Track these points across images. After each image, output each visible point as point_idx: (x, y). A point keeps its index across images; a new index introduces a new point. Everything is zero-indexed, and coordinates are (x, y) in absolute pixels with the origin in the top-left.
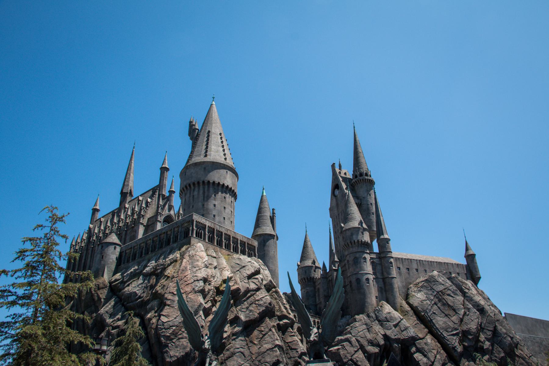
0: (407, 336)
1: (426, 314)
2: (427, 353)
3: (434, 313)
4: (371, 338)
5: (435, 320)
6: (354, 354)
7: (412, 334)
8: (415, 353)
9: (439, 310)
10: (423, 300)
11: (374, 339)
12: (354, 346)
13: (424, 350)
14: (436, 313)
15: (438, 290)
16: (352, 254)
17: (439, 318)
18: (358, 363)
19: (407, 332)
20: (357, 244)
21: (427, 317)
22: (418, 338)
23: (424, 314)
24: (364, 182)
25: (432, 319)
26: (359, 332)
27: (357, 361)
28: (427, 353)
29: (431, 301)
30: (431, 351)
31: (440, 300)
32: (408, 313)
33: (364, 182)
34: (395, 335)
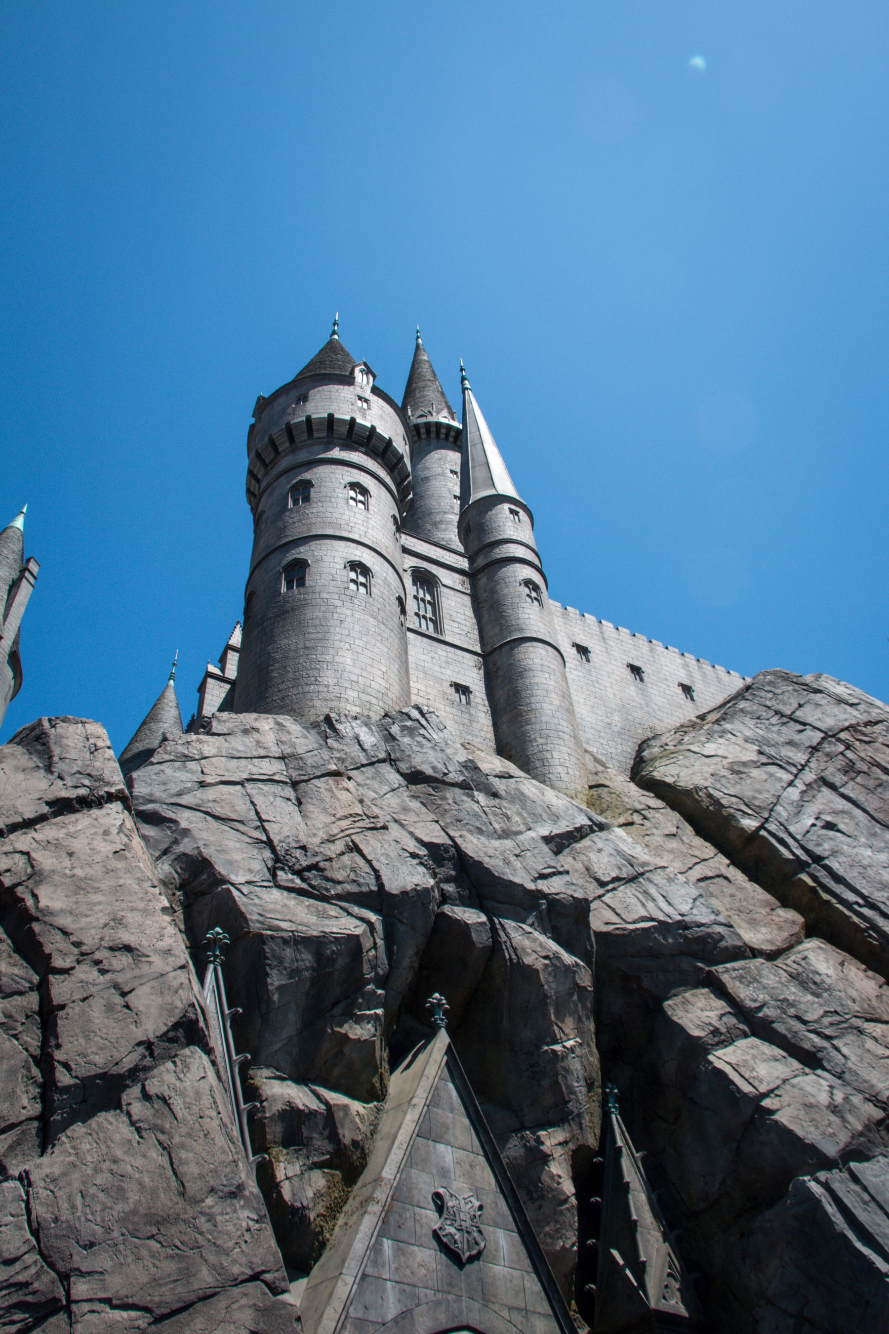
0: (643, 919)
1: (772, 827)
2: (828, 1038)
3: (829, 826)
4: (313, 842)
5: (842, 859)
6: (28, 824)
7: (685, 908)
8: (724, 1039)
9: (858, 812)
10: (744, 764)
11: (339, 846)
12: (59, 767)
13: (799, 1018)
14: (841, 826)
15: (828, 723)
16: (283, 478)
17: (869, 852)
18: (42, 892)
19: (646, 892)
20: (324, 434)
21: (782, 841)
22: (730, 942)
23: (762, 827)
24: (433, 435)
25: (818, 851)
26: (202, 784)
27: (36, 875)
28: (828, 1038)
29: (794, 771)
30: (861, 1032)
31: (850, 769)
32: (645, 818)
33: (433, 435)
34: (543, 877)
